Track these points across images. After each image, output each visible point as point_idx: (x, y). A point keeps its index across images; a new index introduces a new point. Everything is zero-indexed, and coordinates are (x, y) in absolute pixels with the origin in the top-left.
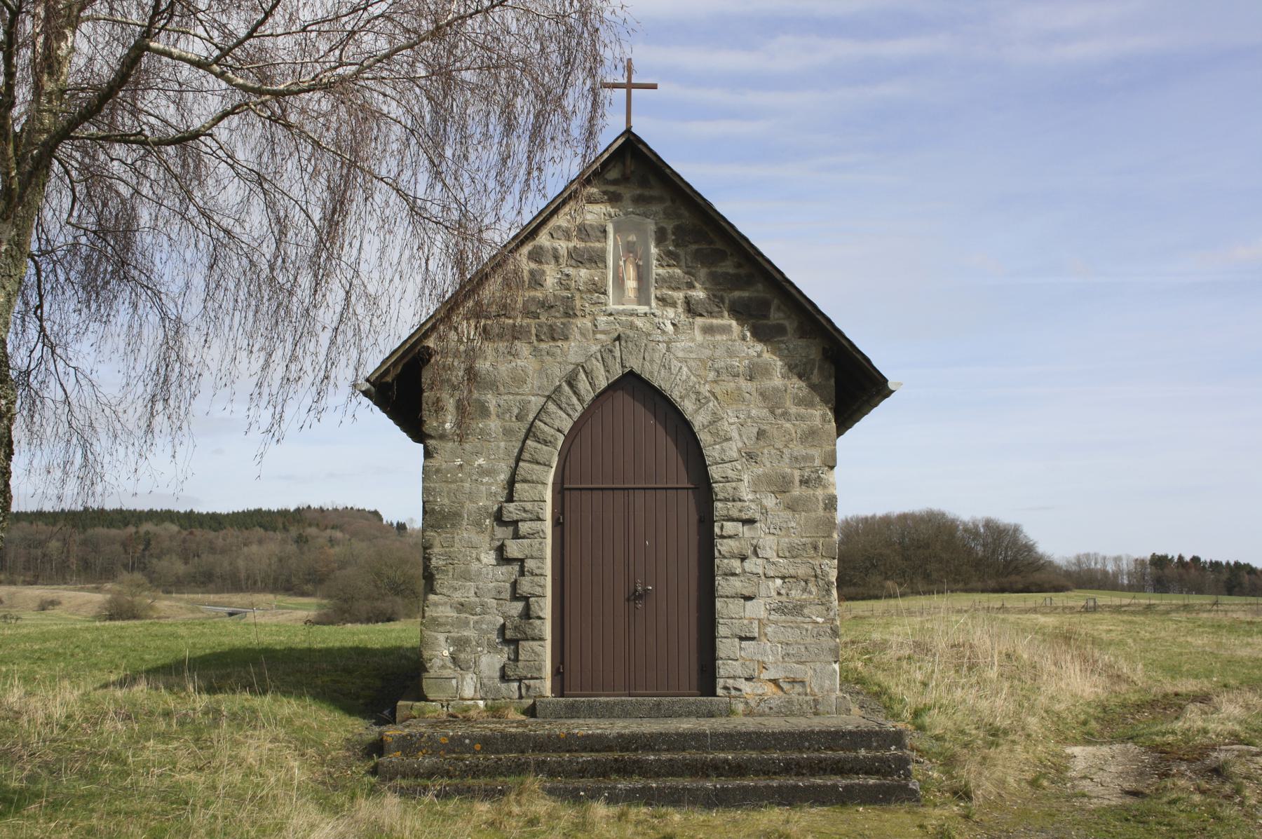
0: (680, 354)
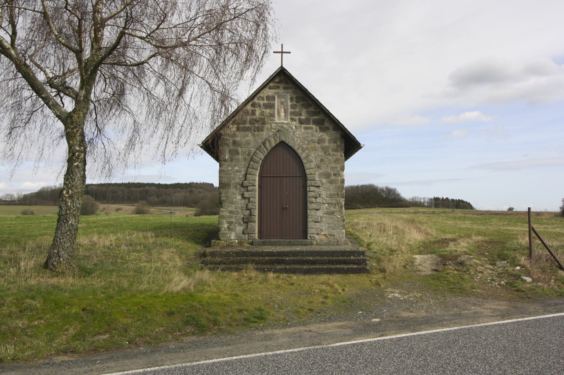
0: (297, 136)
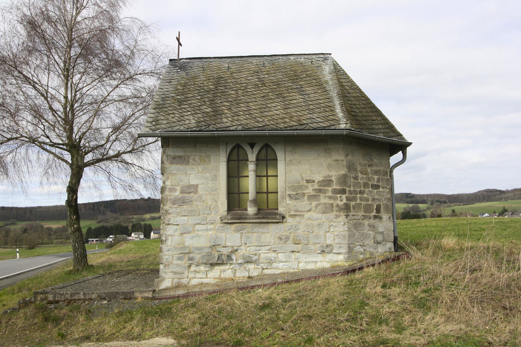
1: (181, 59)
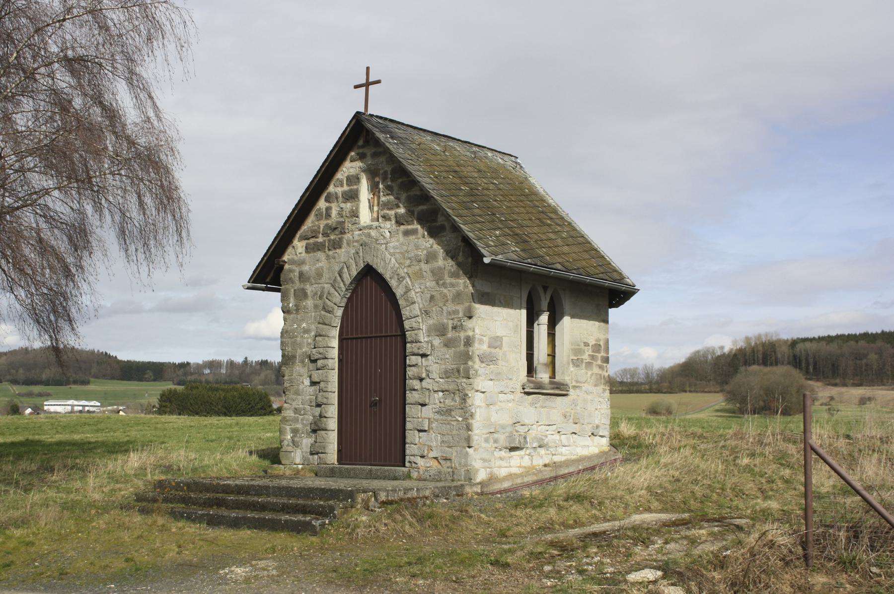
0: (392, 251)
1: (372, 116)
